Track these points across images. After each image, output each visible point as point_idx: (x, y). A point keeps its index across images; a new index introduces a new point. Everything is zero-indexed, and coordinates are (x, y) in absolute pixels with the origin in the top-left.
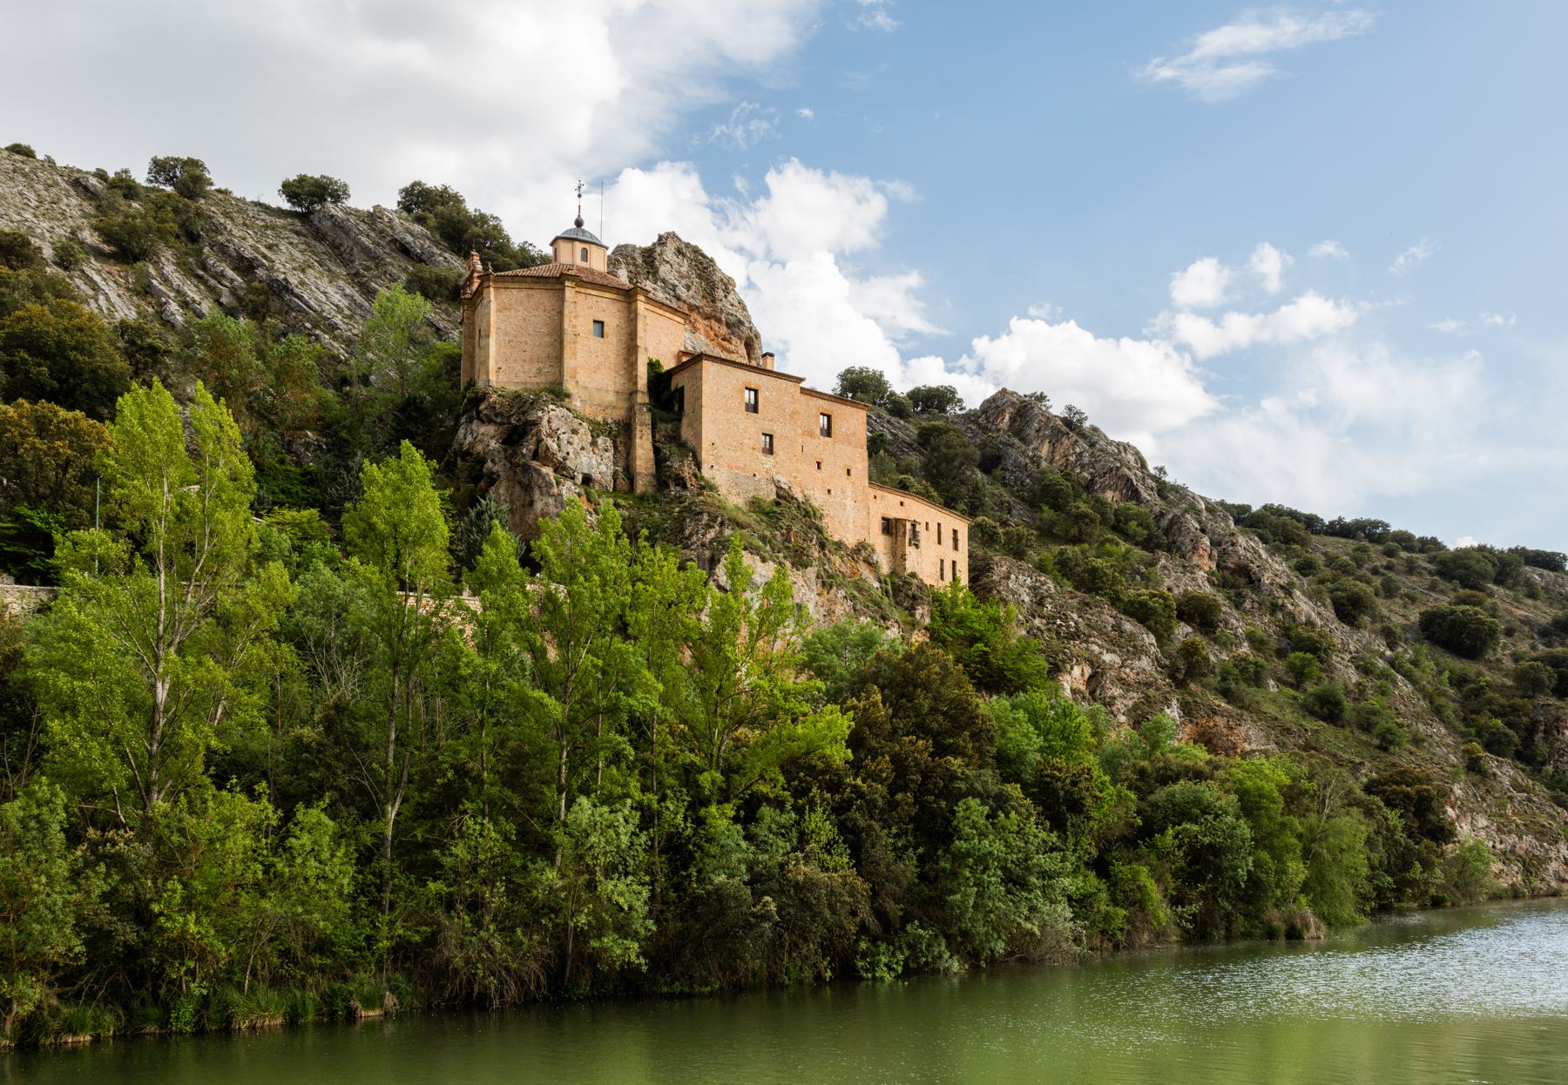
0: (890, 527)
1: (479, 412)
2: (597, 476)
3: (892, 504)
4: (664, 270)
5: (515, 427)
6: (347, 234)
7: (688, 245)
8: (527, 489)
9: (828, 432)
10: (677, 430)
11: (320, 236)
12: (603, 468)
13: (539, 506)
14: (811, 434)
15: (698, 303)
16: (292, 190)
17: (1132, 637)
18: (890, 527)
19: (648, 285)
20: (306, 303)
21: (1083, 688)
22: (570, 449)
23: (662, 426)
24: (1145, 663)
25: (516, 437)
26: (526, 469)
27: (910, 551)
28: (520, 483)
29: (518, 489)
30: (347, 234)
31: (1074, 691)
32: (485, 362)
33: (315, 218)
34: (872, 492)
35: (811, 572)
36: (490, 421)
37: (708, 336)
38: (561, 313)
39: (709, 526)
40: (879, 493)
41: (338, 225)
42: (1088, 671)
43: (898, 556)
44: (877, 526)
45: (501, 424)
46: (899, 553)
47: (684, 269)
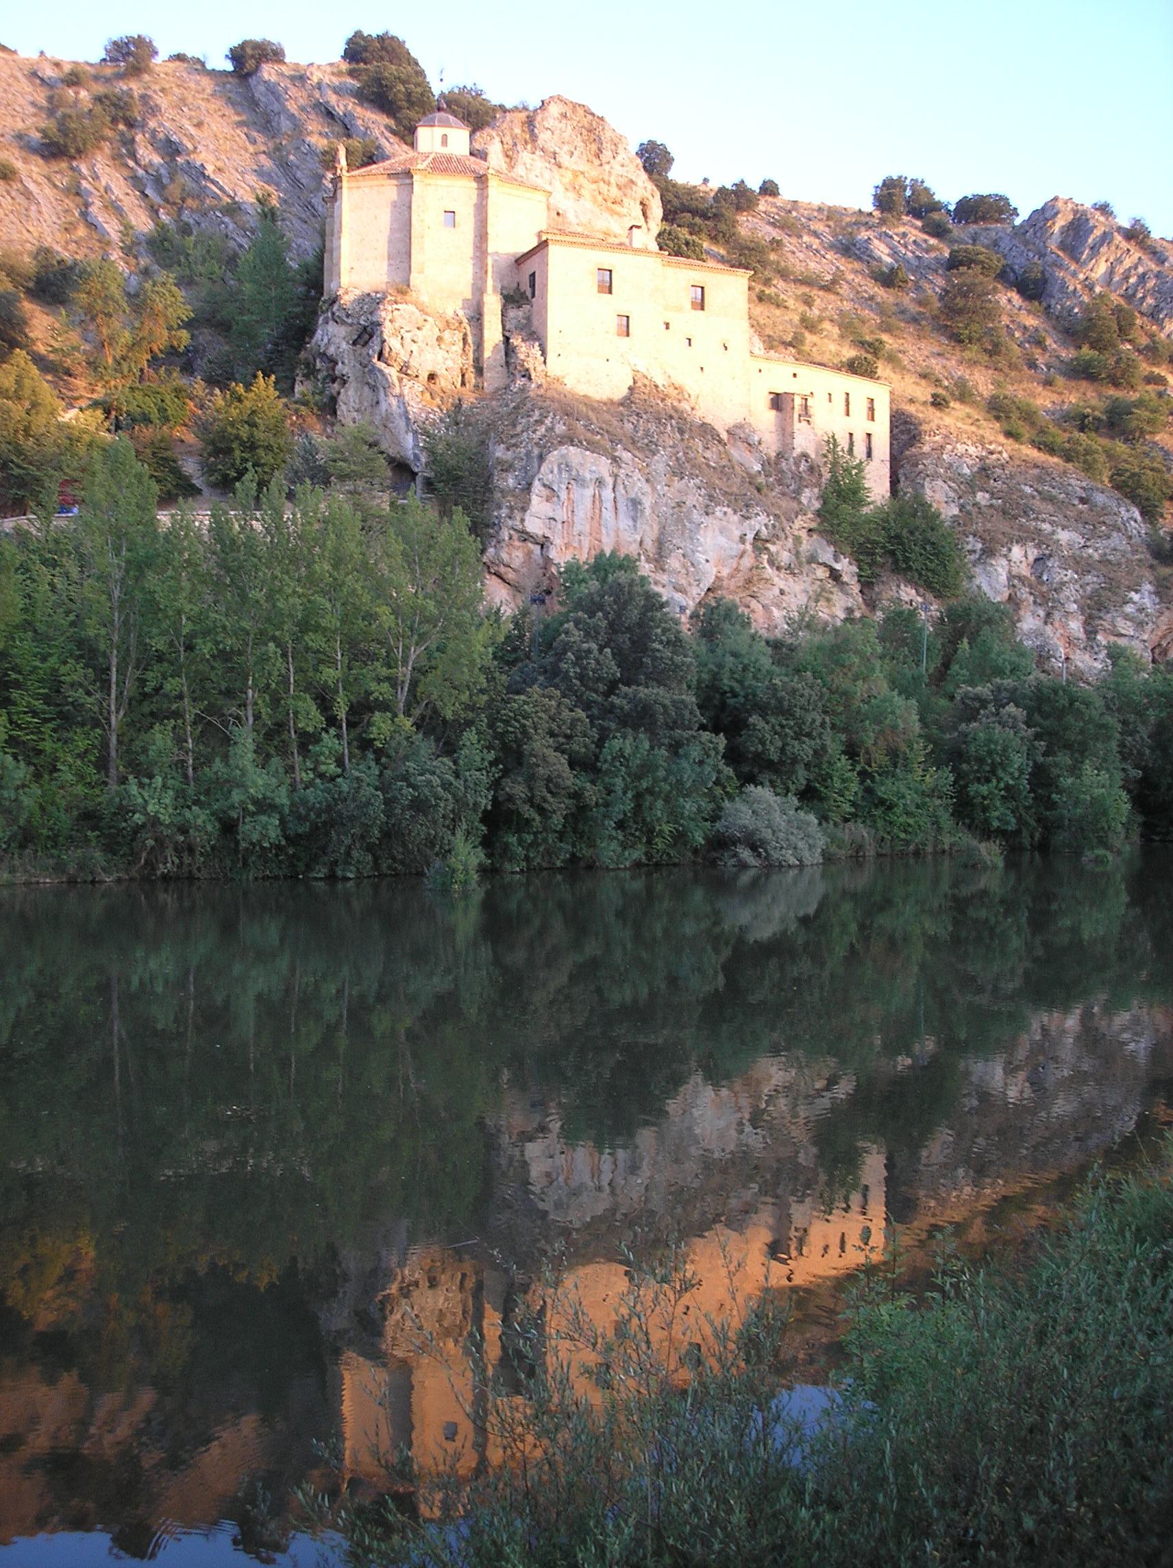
0: (778, 402)
1: (333, 314)
2: (440, 370)
3: (783, 374)
4: (543, 137)
5: (365, 328)
6: (278, 100)
7: (575, 106)
8: (374, 389)
9: (701, 305)
10: (529, 319)
11: (253, 103)
12: (450, 363)
13: (383, 406)
14: (679, 309)
15: (581, 168)
16: (237, 55)
17: (1105, 511)
18: (778, 402)
19: (525, 156)
20: (221, 189)
21: (1025, 571)
22: (414, 347)
23: (512, 313)
24: (1116, 540)
25: (366, 337)
26: (374, 370)
27: (799, 427)
28: (368, 383)
29: (366, 388)
30: (278, 100)
31: (1011, 576)
32: (338, 264)
33: (252, 81)
34: (755, 364)
35: (660, 463)
36: (344, 323)
37: (595, 201)
38: (410, 207)
39: (540, 422)
40: (764, 365)
41: (271, 89)
42: (1033, 553)
43: (785, 433)
44: (764, 401)
45: (351, 325)
46: (788, 430)
47: (566, 135)
